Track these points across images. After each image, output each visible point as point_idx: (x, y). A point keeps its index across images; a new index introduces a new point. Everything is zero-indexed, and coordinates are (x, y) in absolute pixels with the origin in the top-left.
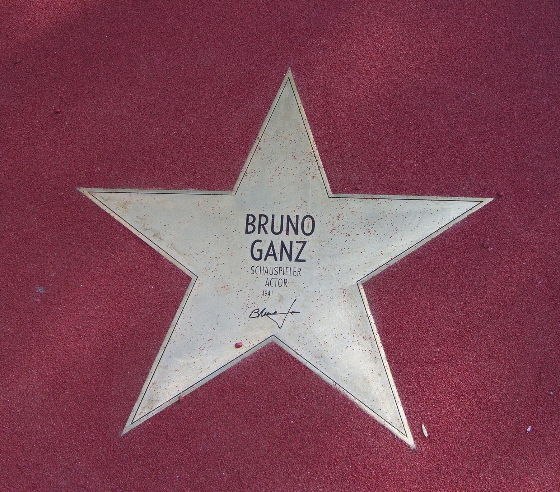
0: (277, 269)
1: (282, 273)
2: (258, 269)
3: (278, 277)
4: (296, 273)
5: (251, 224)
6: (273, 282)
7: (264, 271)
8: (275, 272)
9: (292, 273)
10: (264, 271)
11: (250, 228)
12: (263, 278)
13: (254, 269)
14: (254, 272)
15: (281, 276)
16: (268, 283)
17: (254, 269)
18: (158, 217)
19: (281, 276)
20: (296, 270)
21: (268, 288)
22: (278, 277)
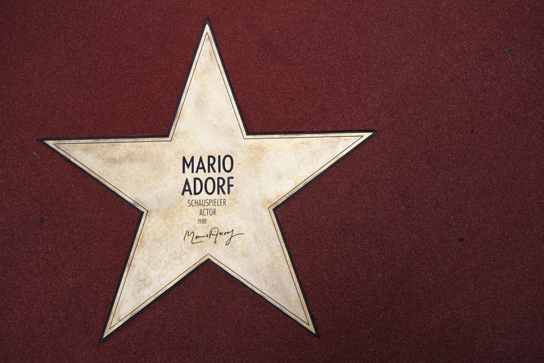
0: (208, 201)
1: (211, 204)
2: (194, 202)
3: (208, 207)
4: (222, 204)
6: (206, 211)
8: (206, 204)
9: (219, 204)
10: (198, 203)
12: (198, 208)
13: (190, 202)
14: (191, 205)
15: (211, 207)
16: (201, 213)
17: (190, 202)
18: (115, 163)
19: (211, 207)
20: (222, 201)
21: (201, 217)
22: (208, 207)
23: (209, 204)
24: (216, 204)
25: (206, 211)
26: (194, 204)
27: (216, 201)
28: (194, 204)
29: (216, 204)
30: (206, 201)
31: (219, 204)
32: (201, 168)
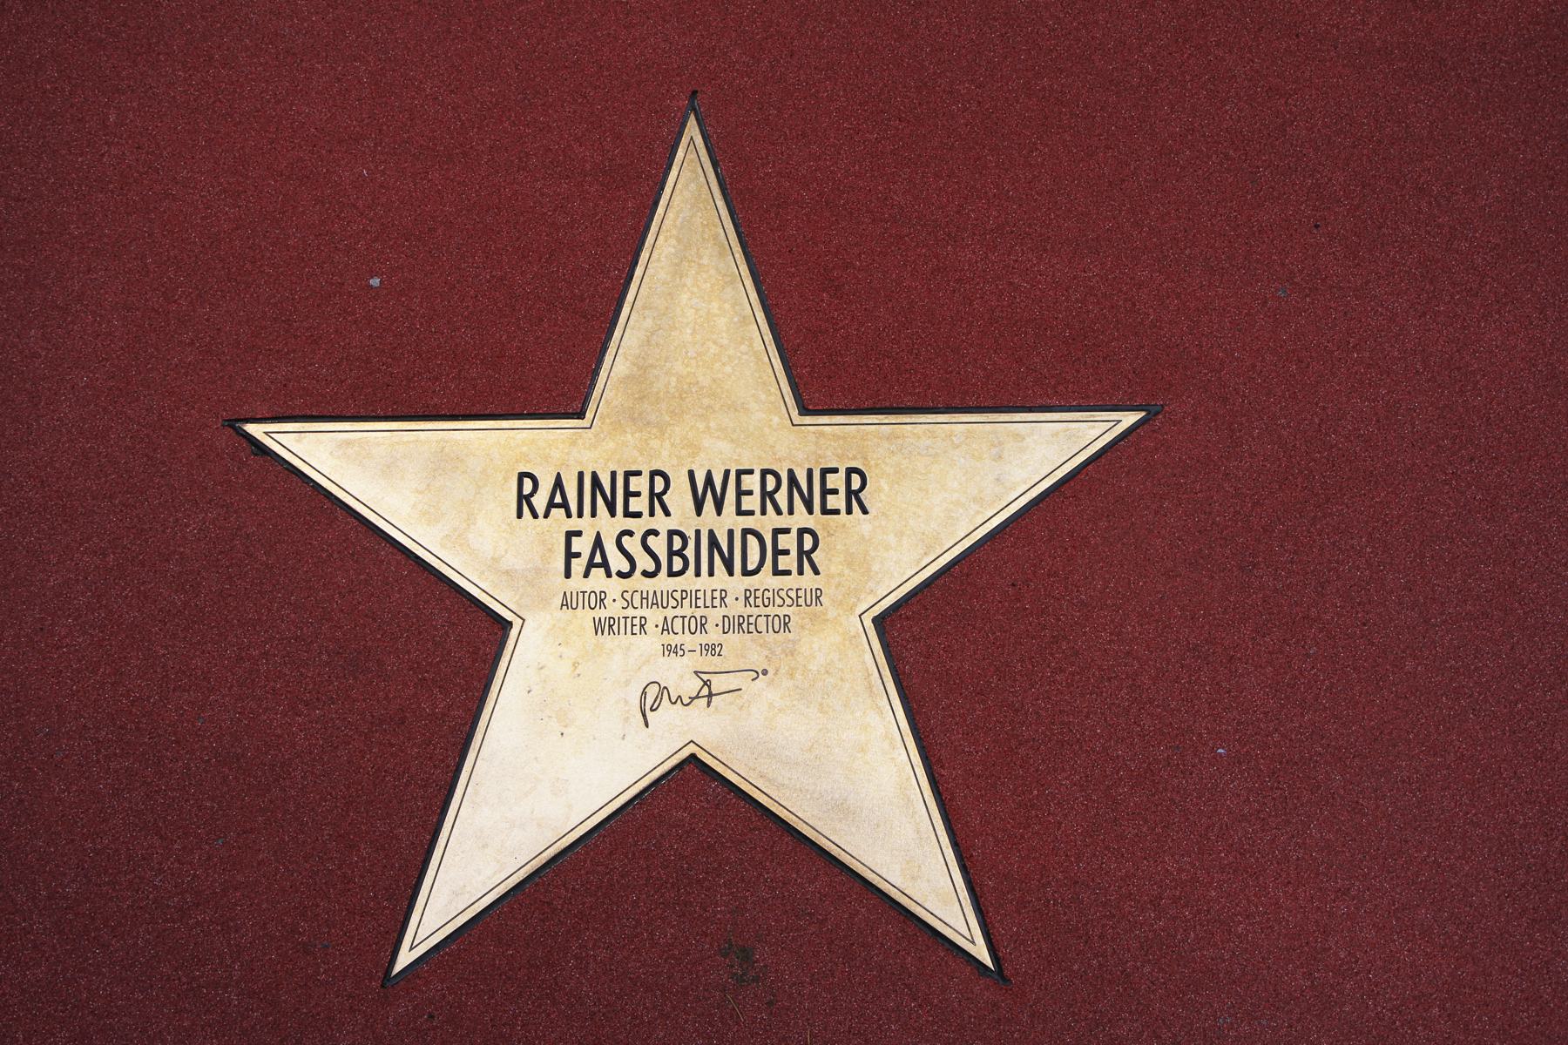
0: (677, 595)
2: (637, 597)
3: (679, 612)
4: (717, 602)
5: (680, 553)
7: (654, 601)
9: (709, 603)
10: (654, 601)
11: (678, 564)
15: (686, 610)
20: (717, 594)
22: (679, 612)
23: (679, 604)
24: (700, 603)
25: (678, 622)
26: (637, 602)
27: (700, 595)
28: (637, 602)
29: (700, 603)
30: (671, 595)
31: (709, 603)
32: (558, 506)
